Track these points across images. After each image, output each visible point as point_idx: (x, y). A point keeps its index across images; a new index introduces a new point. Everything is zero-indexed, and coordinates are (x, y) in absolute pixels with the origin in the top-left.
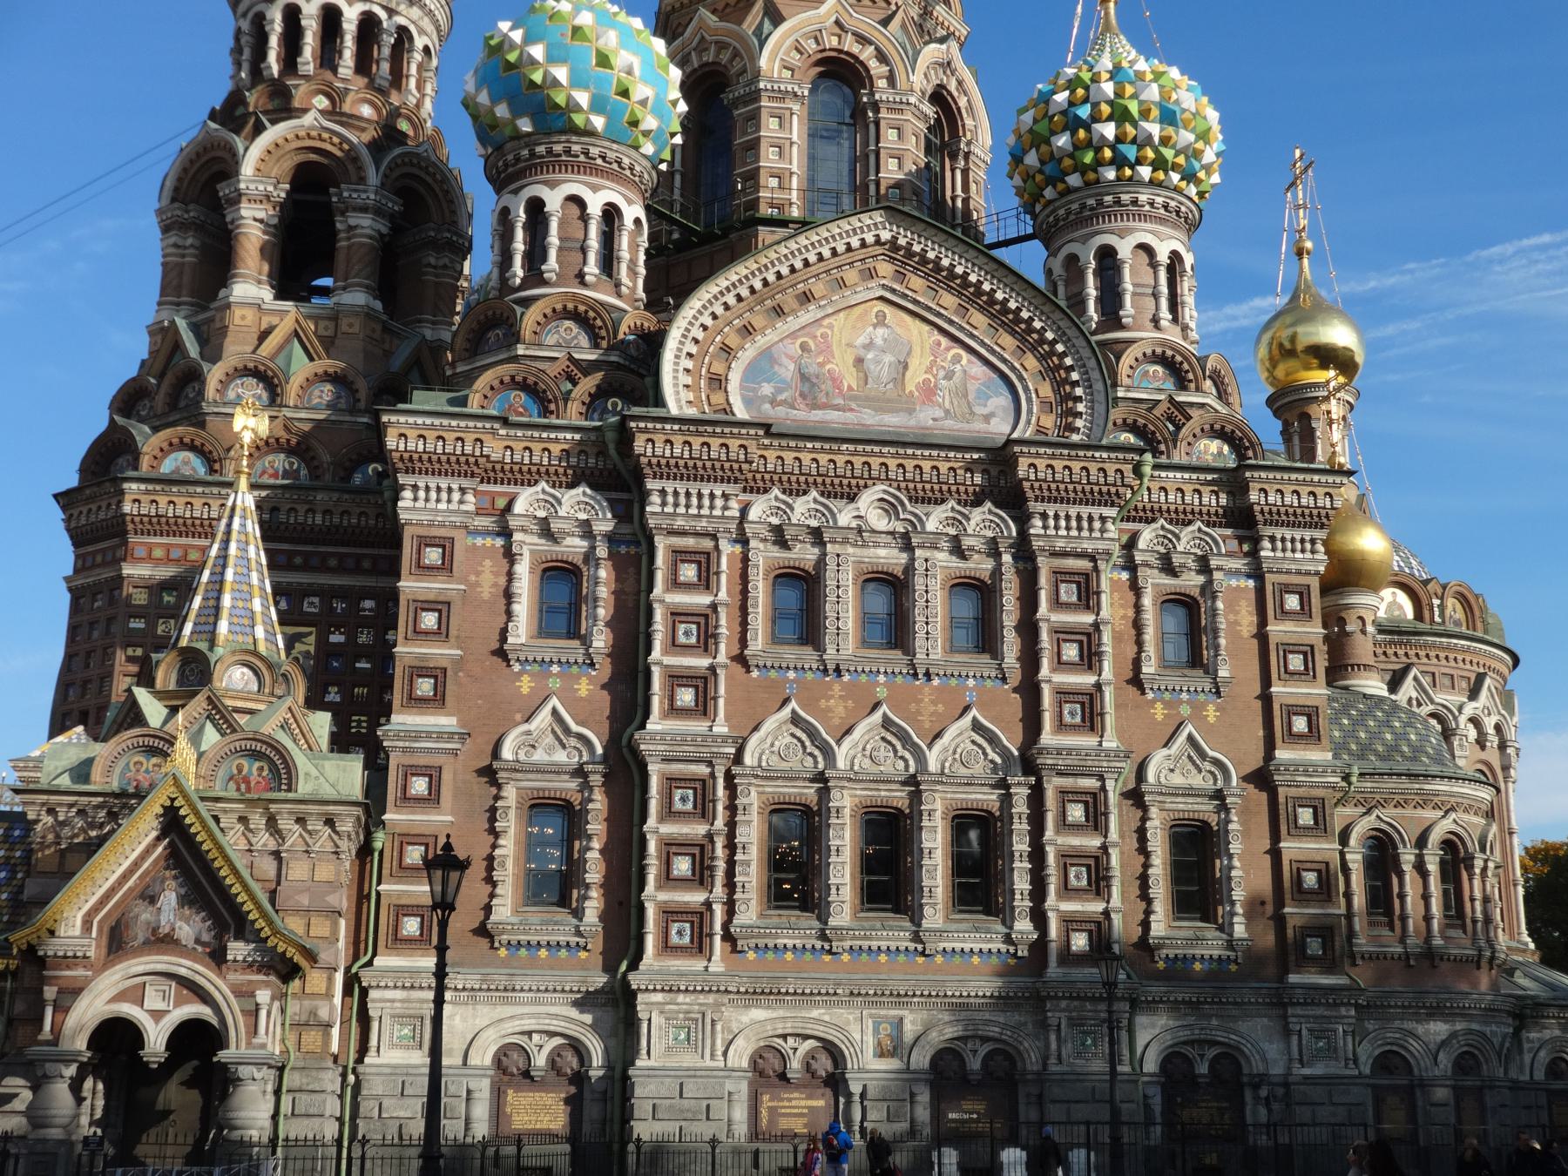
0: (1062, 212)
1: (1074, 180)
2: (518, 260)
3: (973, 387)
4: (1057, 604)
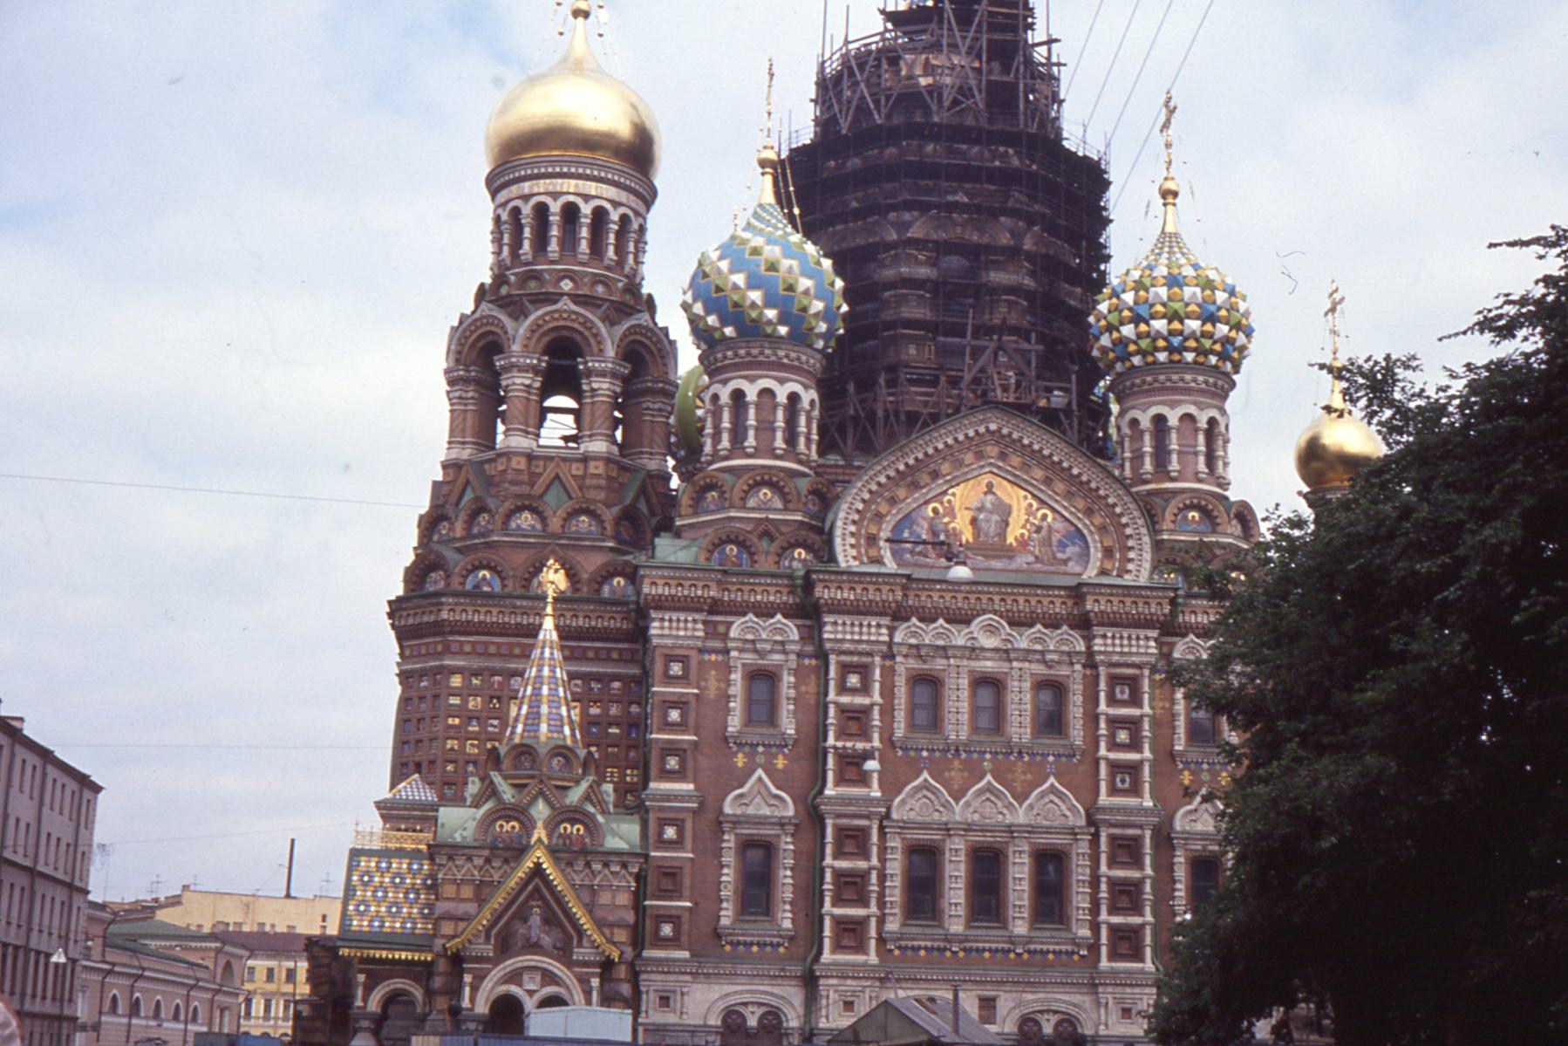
0: (1128, 383)
1: (1136, 360)
2: (725, 437)
3: (1056, 537)
4: (1112, 701)
